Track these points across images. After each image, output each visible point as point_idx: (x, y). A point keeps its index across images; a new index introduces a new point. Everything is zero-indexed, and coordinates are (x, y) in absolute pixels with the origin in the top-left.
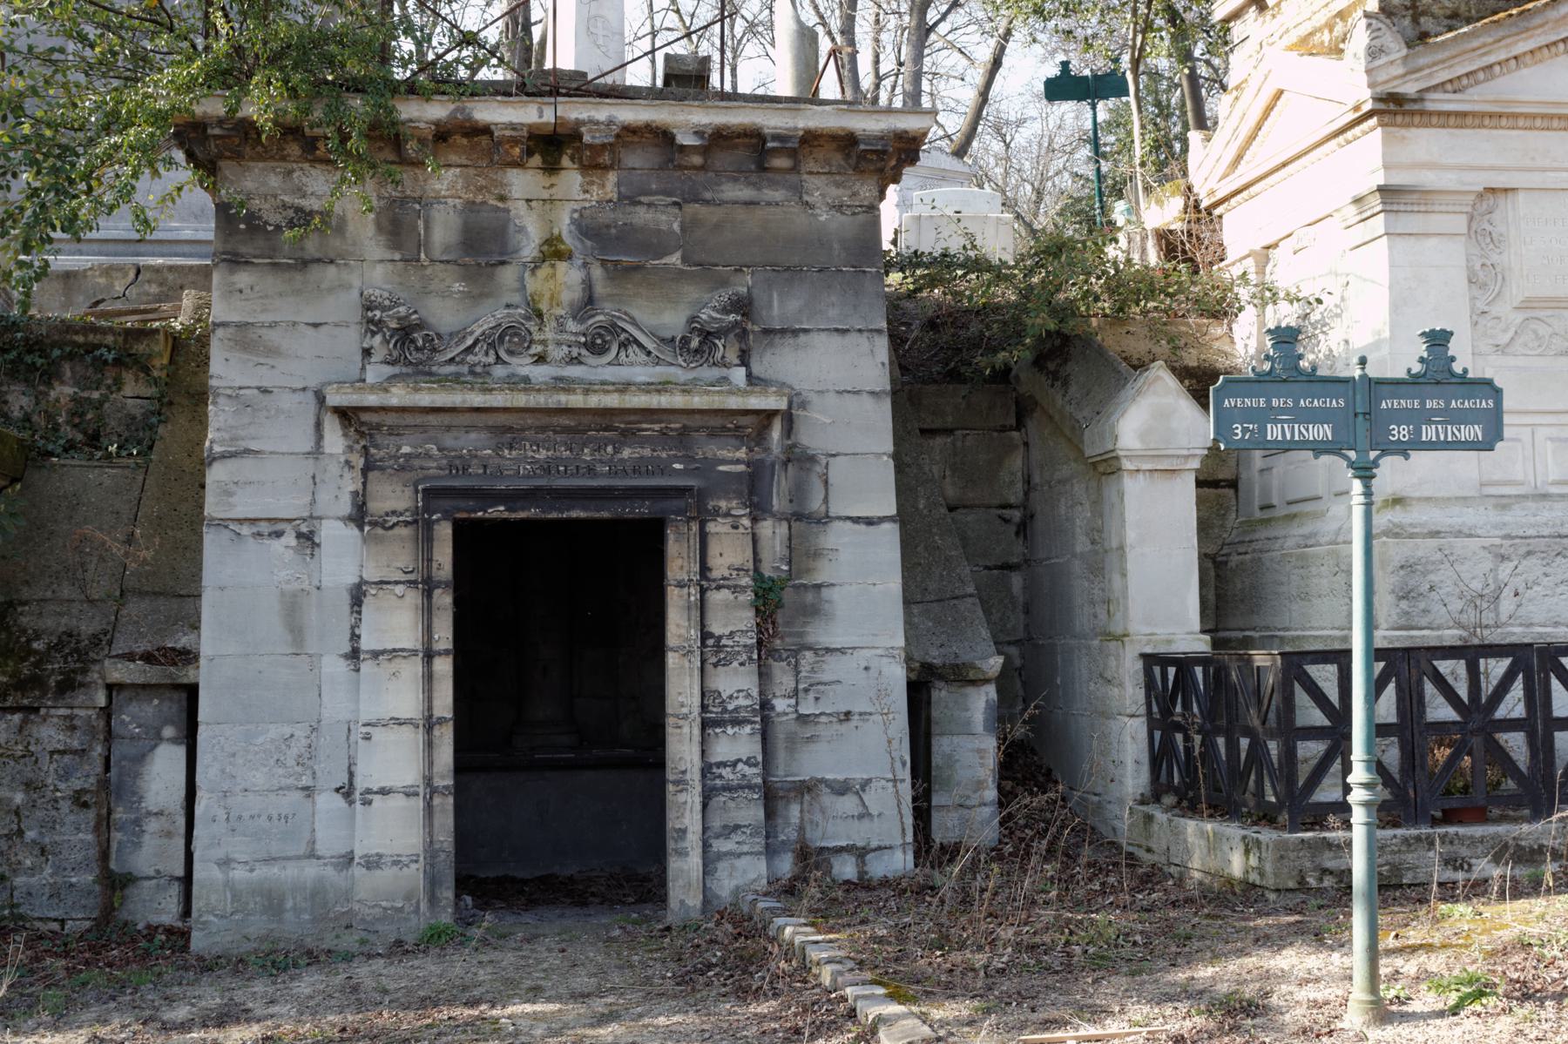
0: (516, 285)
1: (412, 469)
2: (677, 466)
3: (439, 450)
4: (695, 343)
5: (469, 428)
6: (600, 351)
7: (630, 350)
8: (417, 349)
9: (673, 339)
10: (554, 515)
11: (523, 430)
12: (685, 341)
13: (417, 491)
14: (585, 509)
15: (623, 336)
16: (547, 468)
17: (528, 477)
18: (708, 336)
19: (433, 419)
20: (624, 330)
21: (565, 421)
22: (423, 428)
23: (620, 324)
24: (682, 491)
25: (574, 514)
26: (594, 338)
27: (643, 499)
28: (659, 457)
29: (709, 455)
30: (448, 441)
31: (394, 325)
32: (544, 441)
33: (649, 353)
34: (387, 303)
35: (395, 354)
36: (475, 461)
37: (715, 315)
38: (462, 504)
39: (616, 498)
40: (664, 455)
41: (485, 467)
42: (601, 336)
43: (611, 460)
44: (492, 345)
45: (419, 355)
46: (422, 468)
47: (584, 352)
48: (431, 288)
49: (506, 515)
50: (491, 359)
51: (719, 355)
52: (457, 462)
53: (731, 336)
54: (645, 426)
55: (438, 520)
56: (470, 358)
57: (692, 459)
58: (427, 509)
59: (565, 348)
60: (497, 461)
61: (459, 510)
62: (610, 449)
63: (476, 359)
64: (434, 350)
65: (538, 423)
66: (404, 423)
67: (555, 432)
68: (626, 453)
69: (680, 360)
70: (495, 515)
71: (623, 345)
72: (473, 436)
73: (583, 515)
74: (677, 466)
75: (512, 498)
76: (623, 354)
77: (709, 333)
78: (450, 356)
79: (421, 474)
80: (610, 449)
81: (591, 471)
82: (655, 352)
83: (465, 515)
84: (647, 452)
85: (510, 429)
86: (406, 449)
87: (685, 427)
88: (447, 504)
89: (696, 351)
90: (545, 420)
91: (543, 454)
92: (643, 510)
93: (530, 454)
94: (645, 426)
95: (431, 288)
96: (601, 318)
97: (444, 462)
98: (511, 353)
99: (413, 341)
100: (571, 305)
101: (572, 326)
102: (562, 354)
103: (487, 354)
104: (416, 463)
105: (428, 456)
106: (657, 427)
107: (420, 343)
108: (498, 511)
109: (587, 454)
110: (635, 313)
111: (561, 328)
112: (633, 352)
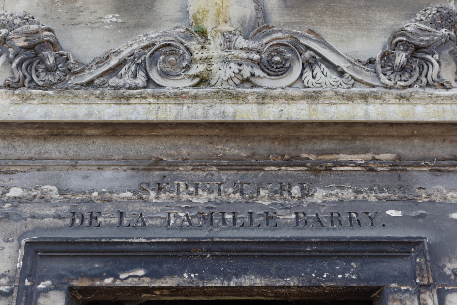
0: (179, 15)
1: (20, 217)
2: (392, 213)
3: (61, 192)
4: (401, 58)
5: (102, 163)
6: (276, 69)
7: (317, 70)
8: (48, 70)
9: (371, 62)
10: (217, 282)
11: (175, 165)
12: (387, 57)
13: (20, 247)
14: (261, 273)
15: (307, 54)
16: (208, 217)
17: (182, 228)
18: (417, 51)
19: (53, 149)
20: (308, 48)
21: (234, 150)
22: (39, 163)
23: (303, 41)
24: (405, 247)
25: (246, 281)
26: (270, 55)
27: (348, 259)
28: (364, 200)
29: (437, 198)
30: (75, 180)
31: (21, 42)
32: (205, 180)
33: (342, 73)
34: (17, 21)
35: (18, 74)
36: (109, 206)
37: (422, 26)
38: (83, 266)
39: (310, 257)
40: (372, 198)
41: (121, 214)
42: (279, 53)
43: (298, 206)
44: (141, 66)
45: (50, 77)
46: (34, 217)
47: (258, 72)
48: (79, 19)
49: (146, 282)
50: (141, 80)
51: (433, 72)
52: (84, 208)
53: (446, 52)
54: (343, 157)
55: (46, 290)
56: (114, 81)
57: (413, 202)
58: (30, 271)
59: (235, 68)
60: (139, 206)
61: (79, 275)
62: (296, 190)
63: (121, 82)
64: (69, 72)
65: (195, 153)
66: (14, 154)
67: (221, 168)
68: (319, 195)
69: (384, 79)
70: (130, 283)
71: (308, 64)
72: (108, 174)
73: (259, 282)
74: (392, 213)
75: (156, 255)
76: (308, 74)
77: (418, 48)
78: (88, 78)
79: (31, 224)
80: (296, 190)
81: (270, 218)
82: (350, 72)
83: (86, 283)
84: (348, 194)
85: (156, 164)
86: (15, 192)
87: (399, 158)
88: (61, 266)
89: (403, 69)
90: (204, 148)
91: (203, 198)
92: (348, 275)
93: (185, 197)
94: (343, 157)
95: (79, 19)
96: (279, 35)
97: (66, 208)
98: (165, 74)
99: (42, 61)
100: (242, 22)
101: (241, 42)
102: (229, 73)
103: (135, 77)
104: (27, 209)
105: (44, 199)
106: (360, 158)
107: (51, 61)
108: (134, 277)
109: (264, 198)
110: (323, 30)
111: (228, 38)
112: (324, 77)
